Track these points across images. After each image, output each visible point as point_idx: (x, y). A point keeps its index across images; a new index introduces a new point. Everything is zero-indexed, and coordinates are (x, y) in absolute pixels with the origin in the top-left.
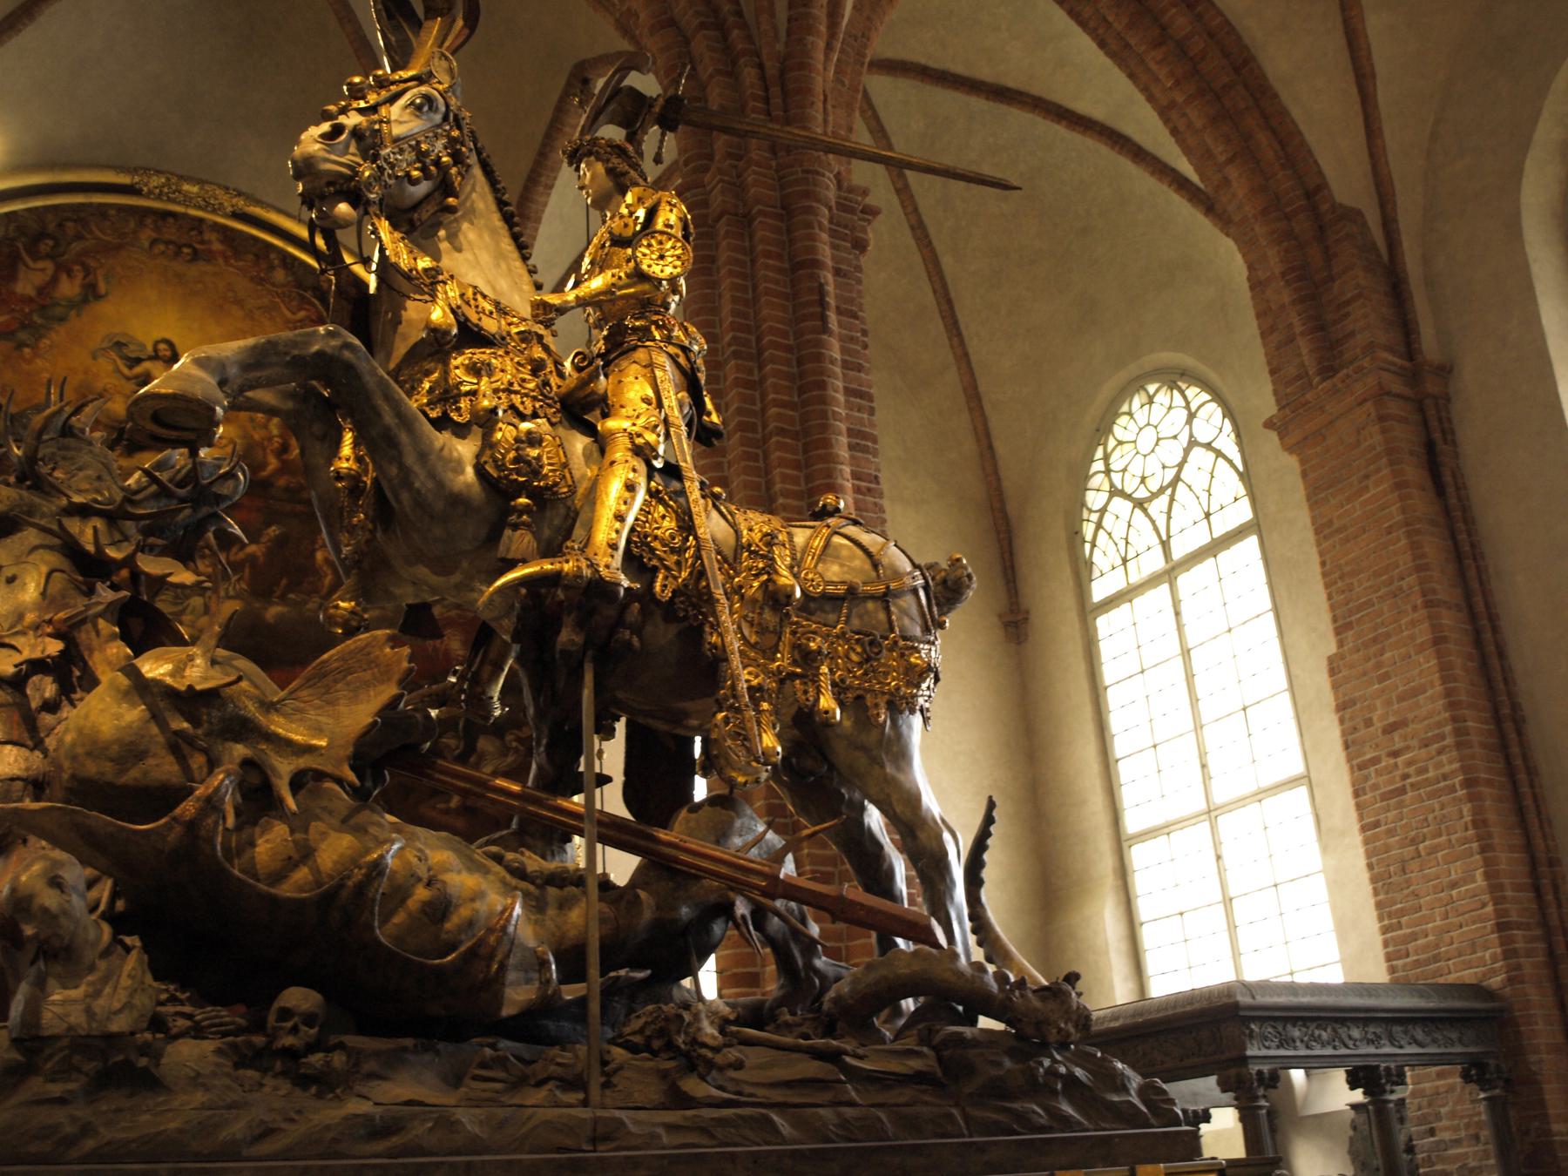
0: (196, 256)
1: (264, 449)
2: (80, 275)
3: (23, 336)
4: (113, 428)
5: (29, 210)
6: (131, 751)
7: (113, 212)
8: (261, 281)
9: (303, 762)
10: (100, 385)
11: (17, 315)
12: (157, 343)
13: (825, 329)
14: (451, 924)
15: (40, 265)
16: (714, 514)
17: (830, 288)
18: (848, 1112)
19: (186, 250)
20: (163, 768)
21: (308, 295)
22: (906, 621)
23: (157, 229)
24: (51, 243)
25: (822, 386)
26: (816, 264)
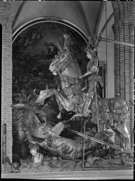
3: (34, 45)
5: (33, 26)
7: (43, 24)
12: (50, 43)
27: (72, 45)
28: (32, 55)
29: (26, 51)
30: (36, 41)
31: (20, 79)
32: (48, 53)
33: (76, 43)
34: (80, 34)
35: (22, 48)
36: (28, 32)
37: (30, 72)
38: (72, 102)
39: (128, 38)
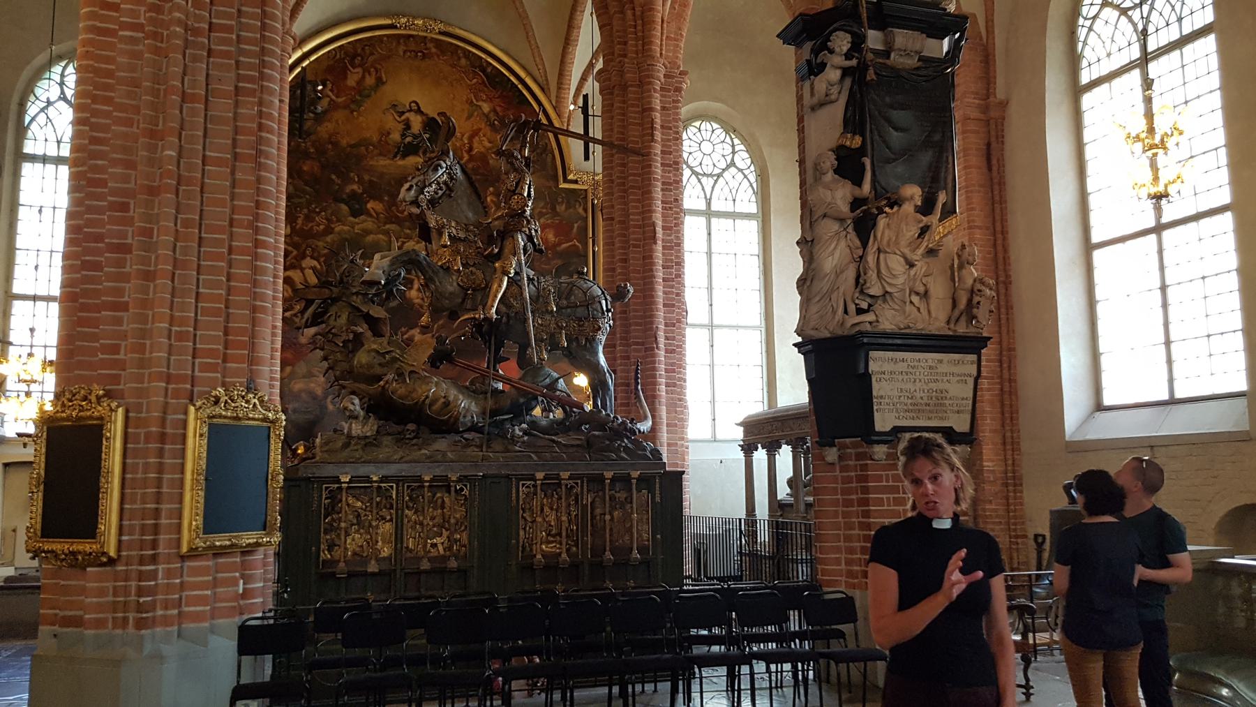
0: (424, 56)
1: (461, 150)
2: (374, 73)
3: (353, 106)
4: (395, 147)
5: (349, 43)
6: (370, 366)
8: (453, 66)
9: (412, 369)
10: (387, 127)
11: (349, 96)
12: (411, 103)
13: (653, 140)
14: (450, 407)
15: (356, 70)
16: (531, 286)
17: (658, 120)
18: (554, 454)
19: (419, 54)
20: (378, 370)
21: (477, 70)
22: (595, 312)
23: (406, 45)
24: (359, 58)
25: (650, 166)
26: (652, 109)
27: (484, 114)
28: (344, 142)
29: (325, 129)
30: (361, 95)
31: (300, 221)
32: (403, 136)
33: (498, 109)
34: (512, 78)
35: (311, 115)
36: (332, 62)
37: (338, 200)
38: (458, 285)
39: (636, 112)
